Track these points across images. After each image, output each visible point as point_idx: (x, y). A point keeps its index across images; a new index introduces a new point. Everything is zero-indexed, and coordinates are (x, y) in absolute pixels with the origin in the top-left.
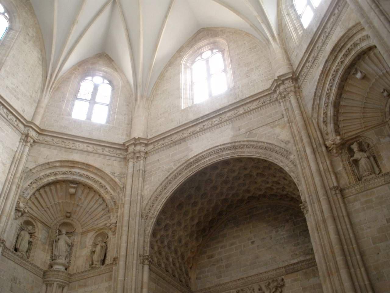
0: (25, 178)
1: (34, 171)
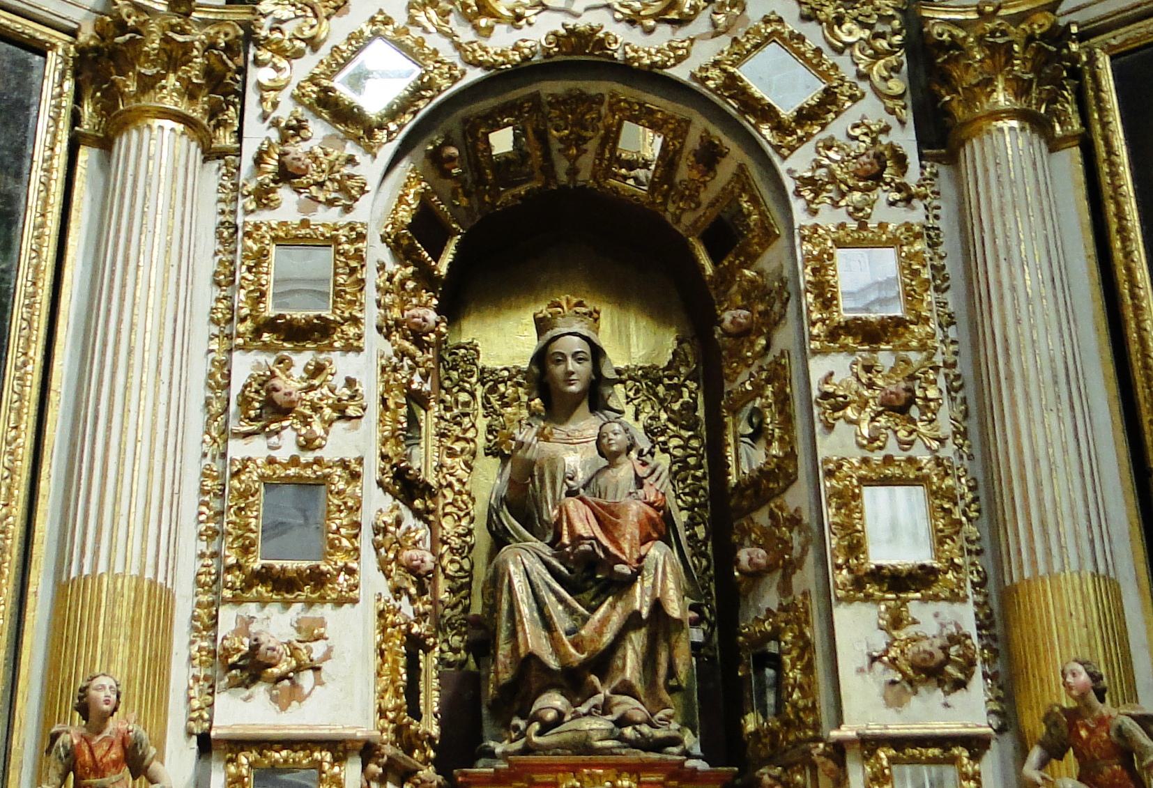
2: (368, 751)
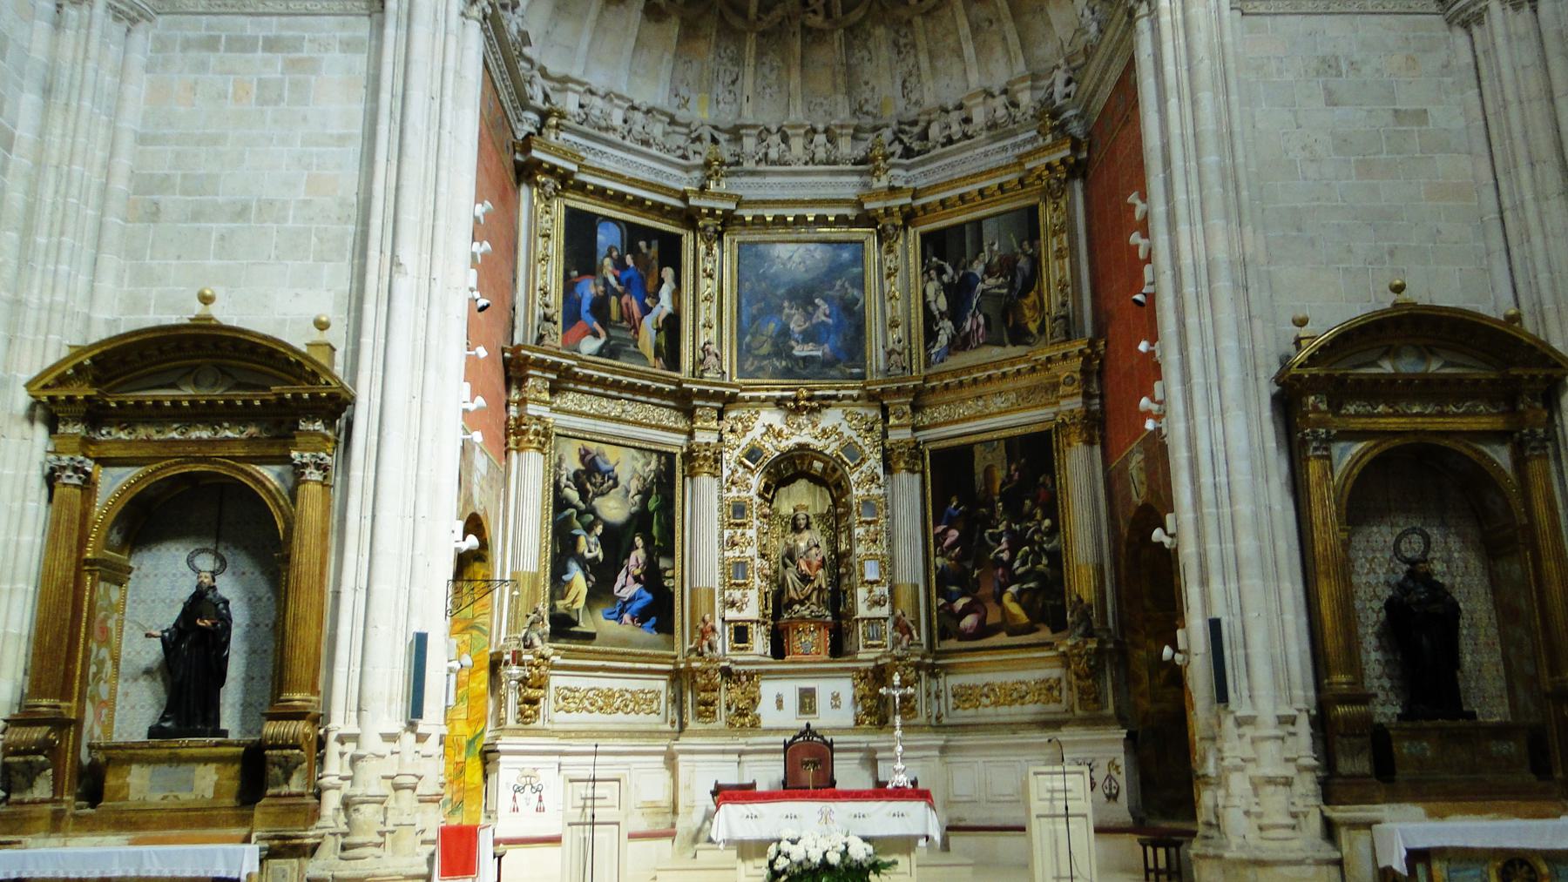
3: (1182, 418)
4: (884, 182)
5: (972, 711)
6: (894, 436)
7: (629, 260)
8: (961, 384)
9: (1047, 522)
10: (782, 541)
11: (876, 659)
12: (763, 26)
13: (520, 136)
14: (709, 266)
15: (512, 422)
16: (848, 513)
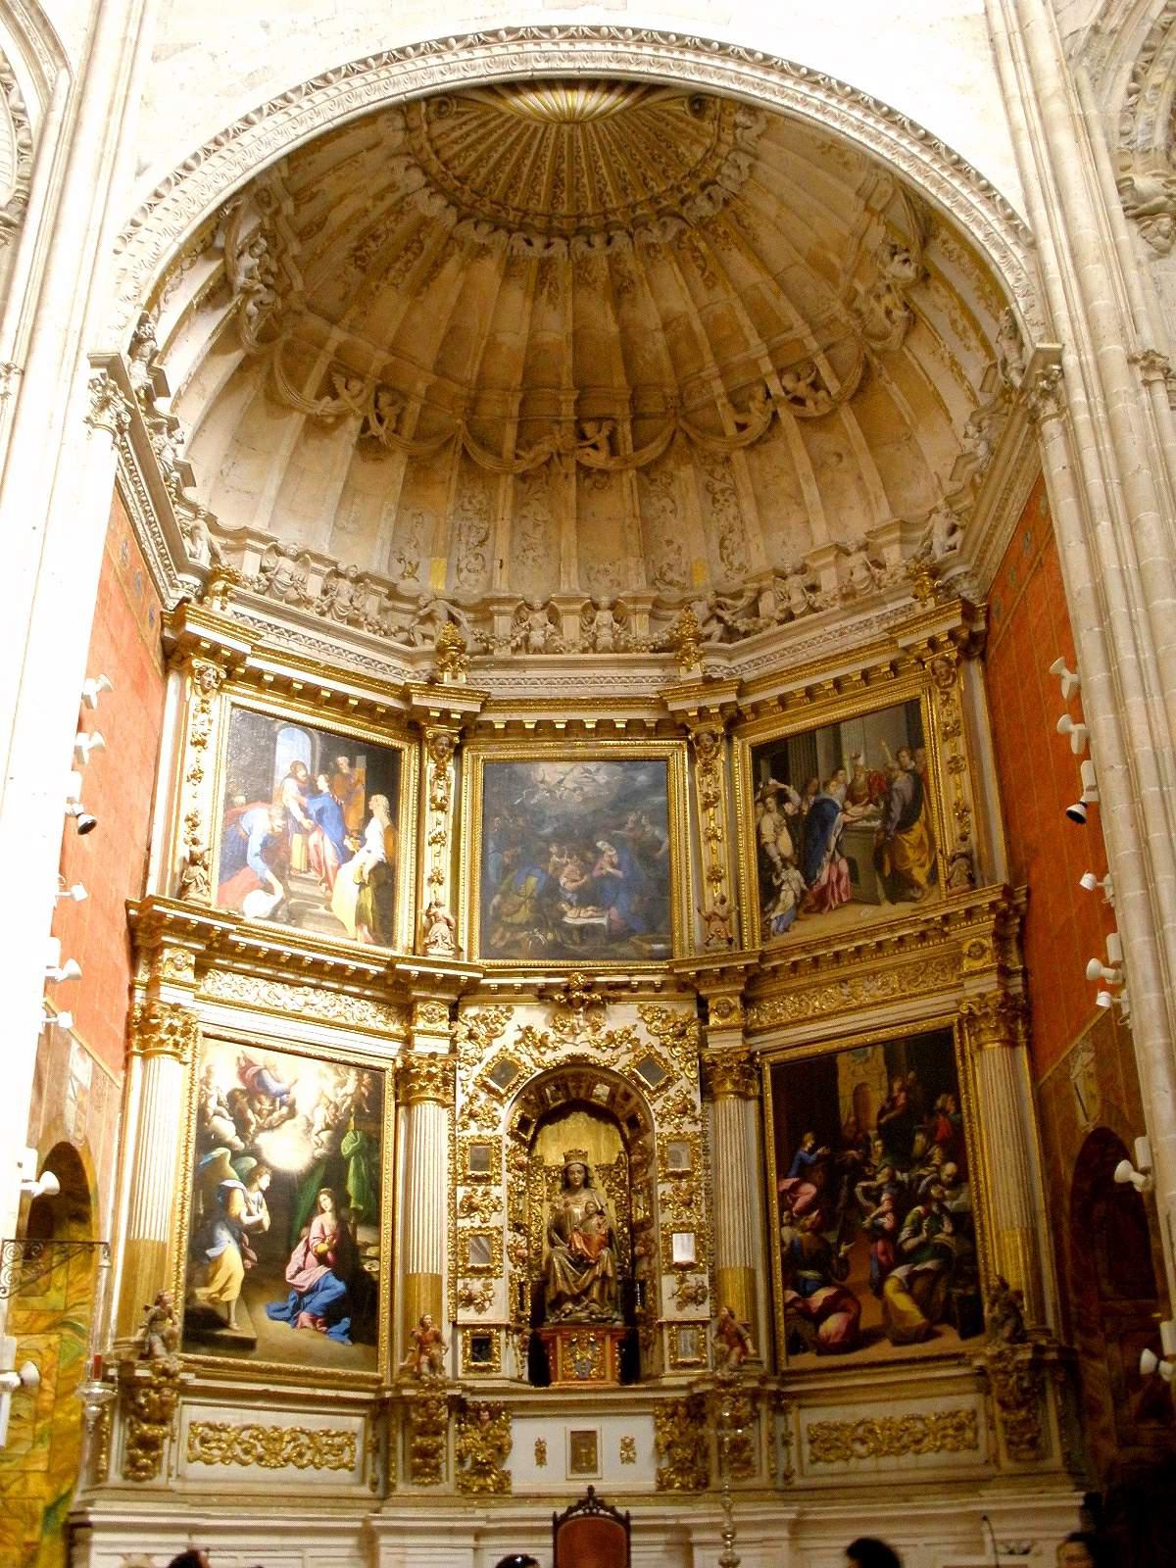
0: (1094, 79)
1: (1114, 21)
2: (507, 1327)
3: (1153, 985)
4: (697, 672)
5: (838, 1466)
6: (716, 1043)
7: (322, 783)
8: (816, 960)
9: (950, 1168)
10: (547, 1205)
11: (690, 1386)
12: (521, 467)
13: (172, 604)
14: (440, 794)
15: (138, 1013)
16: (645, 1163)
